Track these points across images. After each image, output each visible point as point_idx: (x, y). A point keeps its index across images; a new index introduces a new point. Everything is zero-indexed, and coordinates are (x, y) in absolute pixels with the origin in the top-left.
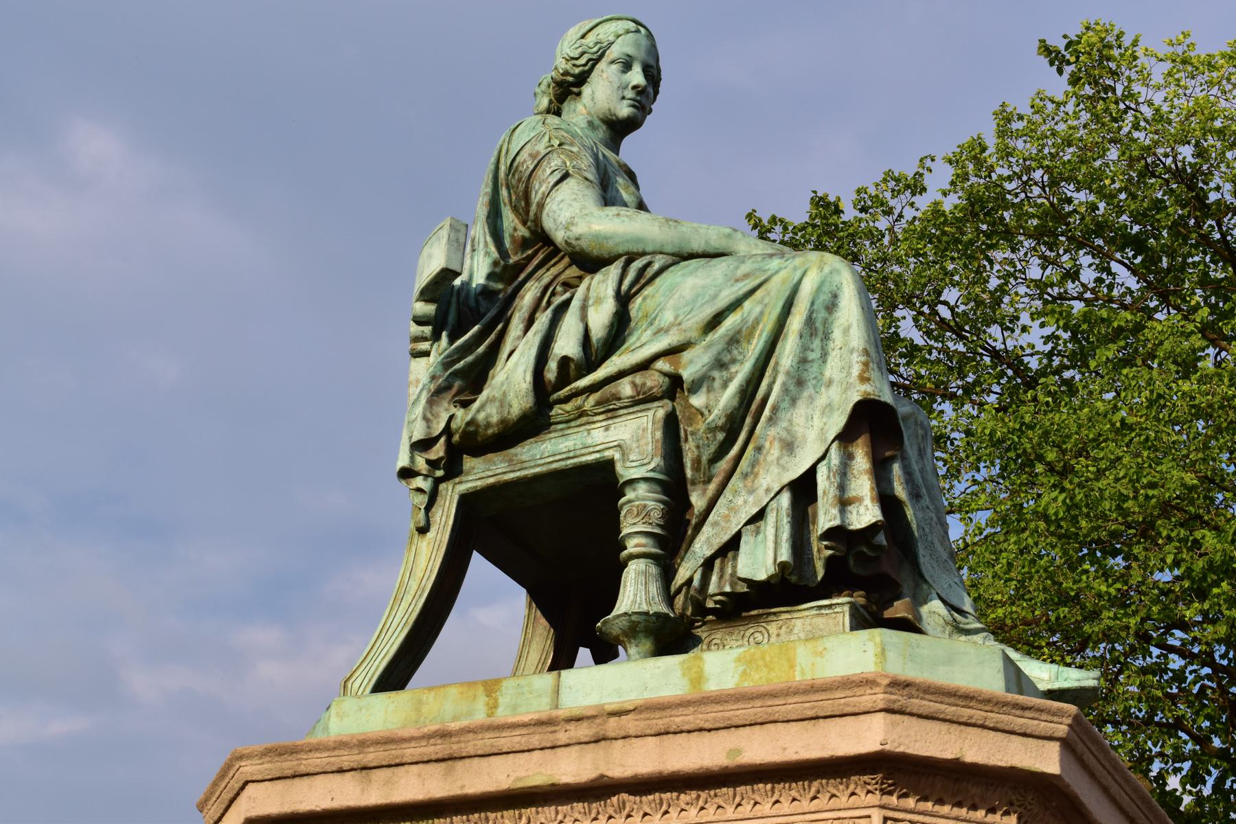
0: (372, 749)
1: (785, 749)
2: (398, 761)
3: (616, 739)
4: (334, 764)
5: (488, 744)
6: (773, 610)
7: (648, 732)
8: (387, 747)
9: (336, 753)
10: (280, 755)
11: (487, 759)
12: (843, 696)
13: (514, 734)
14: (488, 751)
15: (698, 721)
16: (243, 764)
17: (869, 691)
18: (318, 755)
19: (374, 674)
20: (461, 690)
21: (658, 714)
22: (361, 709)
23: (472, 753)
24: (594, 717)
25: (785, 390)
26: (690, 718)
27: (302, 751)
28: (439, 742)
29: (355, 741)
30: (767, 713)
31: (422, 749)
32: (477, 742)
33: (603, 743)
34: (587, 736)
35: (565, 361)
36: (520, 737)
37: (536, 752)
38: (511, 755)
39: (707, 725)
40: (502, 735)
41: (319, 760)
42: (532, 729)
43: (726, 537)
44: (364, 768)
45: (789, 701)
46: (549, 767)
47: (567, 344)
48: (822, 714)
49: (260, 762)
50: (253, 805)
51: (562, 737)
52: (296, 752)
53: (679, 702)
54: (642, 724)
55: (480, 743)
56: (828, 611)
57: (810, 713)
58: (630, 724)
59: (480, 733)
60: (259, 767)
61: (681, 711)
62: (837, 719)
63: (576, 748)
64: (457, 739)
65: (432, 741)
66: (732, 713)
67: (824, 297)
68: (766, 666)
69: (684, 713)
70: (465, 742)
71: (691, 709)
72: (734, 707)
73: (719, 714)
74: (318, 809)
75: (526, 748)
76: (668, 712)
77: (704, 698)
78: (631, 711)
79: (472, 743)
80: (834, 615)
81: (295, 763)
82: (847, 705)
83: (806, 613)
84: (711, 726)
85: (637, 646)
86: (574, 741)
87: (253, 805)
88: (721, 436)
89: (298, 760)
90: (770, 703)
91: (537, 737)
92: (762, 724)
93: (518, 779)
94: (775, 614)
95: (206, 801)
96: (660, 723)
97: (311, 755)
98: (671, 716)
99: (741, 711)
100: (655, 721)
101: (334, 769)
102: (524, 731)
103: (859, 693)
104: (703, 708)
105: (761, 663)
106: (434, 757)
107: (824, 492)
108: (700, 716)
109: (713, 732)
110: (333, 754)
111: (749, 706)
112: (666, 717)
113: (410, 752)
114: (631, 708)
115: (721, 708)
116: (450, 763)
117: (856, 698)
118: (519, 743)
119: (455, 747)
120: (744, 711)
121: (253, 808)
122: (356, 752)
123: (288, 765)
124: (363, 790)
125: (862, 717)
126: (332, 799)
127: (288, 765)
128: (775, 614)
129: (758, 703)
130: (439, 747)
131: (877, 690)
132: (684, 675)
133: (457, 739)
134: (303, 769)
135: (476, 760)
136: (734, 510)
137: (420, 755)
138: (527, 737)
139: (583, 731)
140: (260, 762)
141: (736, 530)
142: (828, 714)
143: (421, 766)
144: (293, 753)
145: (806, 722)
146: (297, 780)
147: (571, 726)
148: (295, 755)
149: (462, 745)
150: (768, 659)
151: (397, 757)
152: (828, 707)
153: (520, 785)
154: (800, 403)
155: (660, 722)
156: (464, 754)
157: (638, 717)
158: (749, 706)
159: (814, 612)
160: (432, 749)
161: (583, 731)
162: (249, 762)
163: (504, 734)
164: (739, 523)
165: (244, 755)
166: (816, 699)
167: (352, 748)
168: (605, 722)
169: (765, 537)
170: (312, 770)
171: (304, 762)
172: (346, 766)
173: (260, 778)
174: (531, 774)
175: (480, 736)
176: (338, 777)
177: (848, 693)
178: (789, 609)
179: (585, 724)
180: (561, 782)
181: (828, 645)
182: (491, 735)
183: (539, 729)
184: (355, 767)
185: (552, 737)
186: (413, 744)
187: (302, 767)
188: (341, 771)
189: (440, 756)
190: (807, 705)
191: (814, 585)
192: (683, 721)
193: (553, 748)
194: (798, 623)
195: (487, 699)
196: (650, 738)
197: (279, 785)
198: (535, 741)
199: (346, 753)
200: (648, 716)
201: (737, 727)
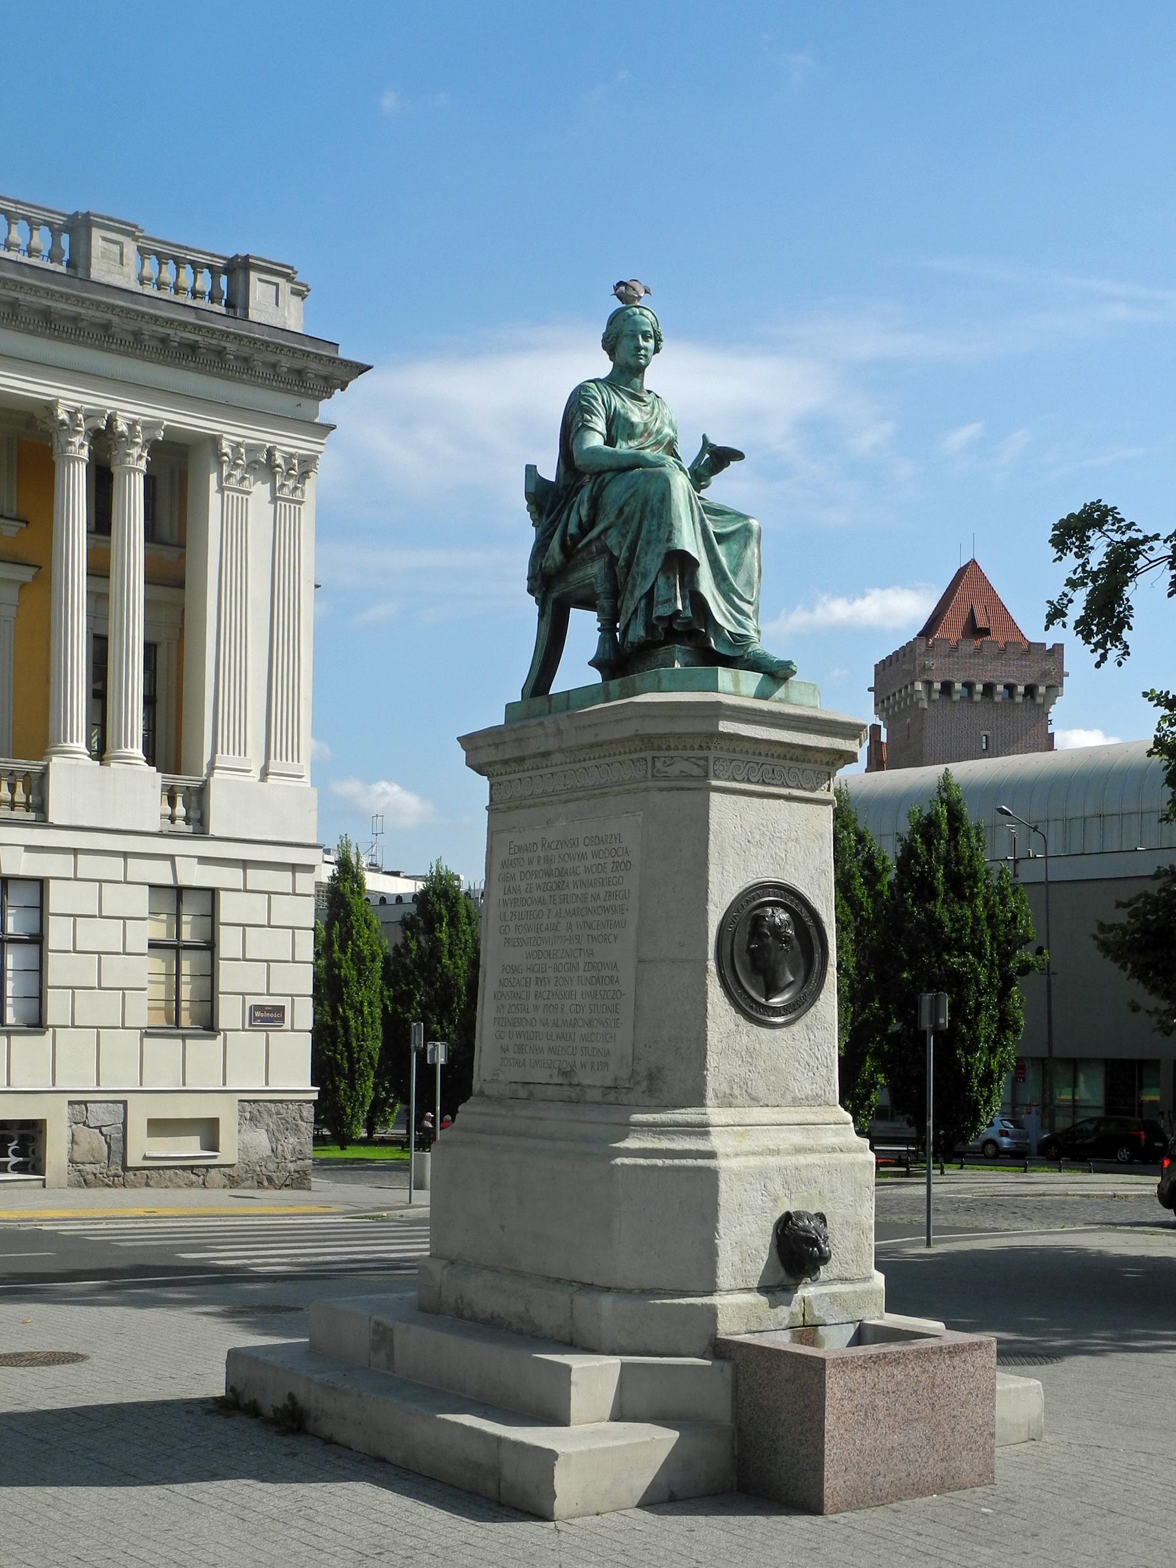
25: (642, 548)
35: (572, 536)
47: (572, 529)
67: (656, 499)
88: (626, 570)
136: (628, 608)
154: (649, 554)
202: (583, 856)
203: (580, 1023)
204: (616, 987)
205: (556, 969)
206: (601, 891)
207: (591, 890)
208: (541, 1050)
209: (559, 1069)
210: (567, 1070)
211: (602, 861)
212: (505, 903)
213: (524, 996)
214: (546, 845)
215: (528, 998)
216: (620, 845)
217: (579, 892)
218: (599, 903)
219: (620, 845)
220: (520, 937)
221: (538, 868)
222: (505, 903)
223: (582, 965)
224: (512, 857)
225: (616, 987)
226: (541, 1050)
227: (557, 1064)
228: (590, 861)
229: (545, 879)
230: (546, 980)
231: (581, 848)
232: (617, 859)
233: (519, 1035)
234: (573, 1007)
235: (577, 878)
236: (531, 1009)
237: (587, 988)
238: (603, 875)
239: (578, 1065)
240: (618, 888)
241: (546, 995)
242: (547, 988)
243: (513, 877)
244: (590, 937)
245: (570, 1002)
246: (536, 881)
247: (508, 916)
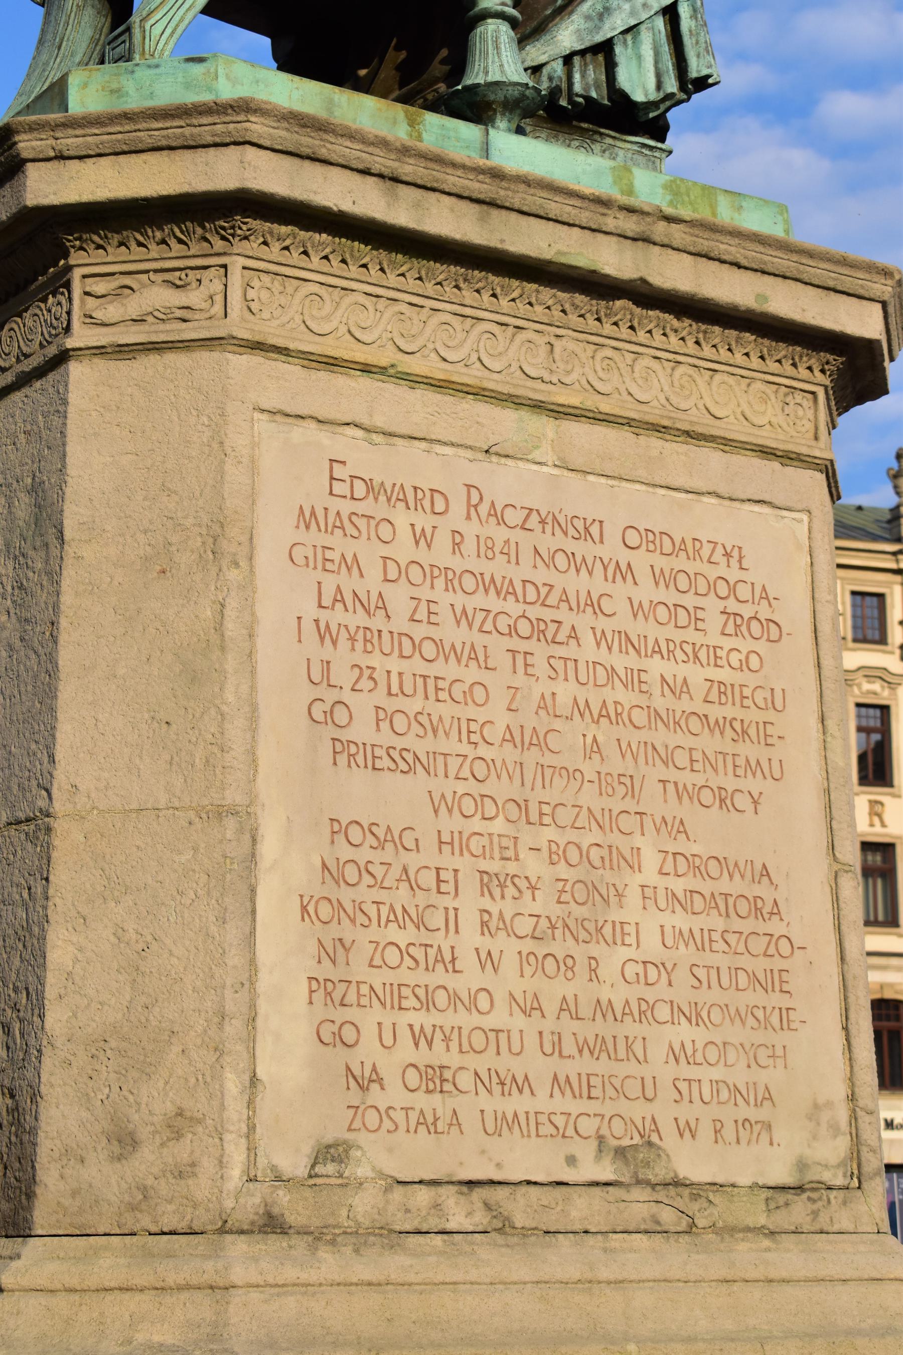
0: (412, 161)
1: (804, 310)
2: (435, 185)
3: (655, 244)
4: (363, 161)
5: (538, 203)
6: (602, 130)
7: (691, 249)
8: (431, 165)
9: (371, 149)
10: (305, 126)
11: (526, 218)
12: (862, 277)
13: (567, 202)
14: (534, 210)
15: (738, 255)
16: (252, 119)
17: (883, 281)
18: (348, 144)
19: (177, 25)
20: (378, 105)
21: (707, 235)
22: (257, 82)
23: (516, 206)
24: (648, 214)
26: (732, 249)
27: (333, 132)
28: (487, 180)
29: (398, 144)
30: (798, 270)
31: (467, 182)
32: (527, 197)
33: (640, 243)
34: (632, 231)
36: (571, 208)
37: (576, 229)
38: (551, 223)
39: (744, 262)
40: (556, 199)
41: (348, 150)
42: (586, 204)
43: (599, 38)
44: (396, 180)
45: (820, 266)
46: (590, 250)
48: (839, 288)
49: (275, 125)
50: (254, 175)
51: (610, 223)
52: (325, 131)
53: (731, 229)
54: (688, 239)
55: (529, 198)
56: (647, 152)
57: (831, 284)
58: (677, 234)
59: (535, 187)
60: (272, 130)
61: (727, 239)
62: (844, 297)
63: (614, 239)
64: (506, 185)
65: (481, 177)
66: (770, 258)
68: (691, 203)
69: (730, 242)
70: (513, 191)
71: (737, 241)
72: (773, 254)
73: (759, 255)
74: (335, 209)
75: (571, 222)
76: (717, 236)
77: (754, 234)
78: (686, 222)
79: (520, 195)
80: (653, 159)
81: (317, 142)
82: (862, 287)
83: (629, 146)
84: (746, 264)
85: (509, 121)
86: (619, 232)
87: (254, 175)
89: (321, 140)
90: (804, 261)
91: (587, 214)
92: (785, 277)
93: (559, 253)
94: (601, 134)
95: (57, 126)
96: (704, 245)
97: (340, 140)
98: (717, 241)
99: (777, 260)
100: (701, 240)
101: (361, 167)
102: (578, 203)
103: (874, 280)
104: (748, 244)
105: (686, 199)
106: (475, 195)
107: (690, 31)
108: (742, 251)
109: (742, 270)
110: (366, 149)
111: (786, 257)
112: (713, 240)
113: (453, 180)
114: (688, 219)
115: (762, 250)
116: (485, 207)
117: (869, 283)
118: (569, 214)
119: (502, 193)
120: (780, 260)
121: (255, 178)
122: (393, 157)
123: (307, 142)
124: (389, 205)
125: (865, 302)
126: (354, 203)
127: (307, 142)
128: (601, 134)
129: (795, 257)
130: (485, 186)
131: (889, 282)
132: (615, 182)
133: (506, 185)
134: (323, 153)
135: (514, 216)
137: (463, 187)
138: (577, 211)
139: (630, 225)
140: (275, 125)
141: (609, 36)
142: (844, 289)
143: (453, 200)
144: (320, 130)
145: (820, 290)
146: (307, 163)
147: (621, 215)
148: (321, 133)
149: (510, 193)
150: (692, 197)
151: (437, 181)
152: (847, 284)
153: (563, 260)
155: (706, 243)
156: (507, 204)
157: (688, 230)
158: (786, 257)
159: (635, 147)
160: (477, 185)
161: (630, 225)
162: (262, 120)
163: (556, 199)
164: (614, 29)
165: (261, 110)
166: (841, 272)
167: (391, 150)
168: (654, 223)
169: (639, 57)
170: (334, 158)
171: (328, 145)
172: (376, 168)
173: (267, 143)
174: (573, 251)
175: (532, 191)
176: (357, 177)
177: (867, 276)
178: (617, 135)
179: (634, 217)
180: (603, 271)
181: (744, 204)
182: (545, 195)
183: (592, 207)
184: (386, 174)
185: (601, 219)
186: (459, 173)
187: (324, 151)
188: (366, 172)
189: (482, 197)
190: (833, 275)
191: (643, 119)
192: (726, 250)
193: (594, 230)
194: (621, 153)
195: (409, 129)
196: (685, 255)
197: (287, 161)
198: (584, 217)
199: (382, 154)
200: (697, 232)
201: (764, 272)
202: (625, 572)
203: (663, 1013)
204: (776, 927)
205: (556, 854)
206: (697, 675)
207: (656, 666)
208: (523, 1085)
209: (601, 1139)
210: (626, 1142)
211: (689, 601)
212: (324, 633)
213: (436, 920)
214: (484, 509)
215: (453, 923)
216: (742, 575)
217: (621, 662)
218: (685, 704)
219: (742, 575)
220: (399, 743)
221: (456, 563)
222: (324, 633)
223: (650, 860)
224: (346, 507)
225: (776, 927)
226: (523, 1085)
227: (588, 1126)
228: (646, 592)
229: (493, 602)
230: (523, 884)
231: (612, 549)
232: (732, 606)
233: (418, 1037)
234: (631, 970)
235: (602, 623)
236: (467, 961)
237: (680, 920)
238: (691, 635)
239: (668, 1129)
240: (752, 680)
241: (524, 926)
242: (528, 905)
243: (352, 565)
244: (671, 787)
245: (624, 953)
246: (450, 597)
247: (343, 676)
